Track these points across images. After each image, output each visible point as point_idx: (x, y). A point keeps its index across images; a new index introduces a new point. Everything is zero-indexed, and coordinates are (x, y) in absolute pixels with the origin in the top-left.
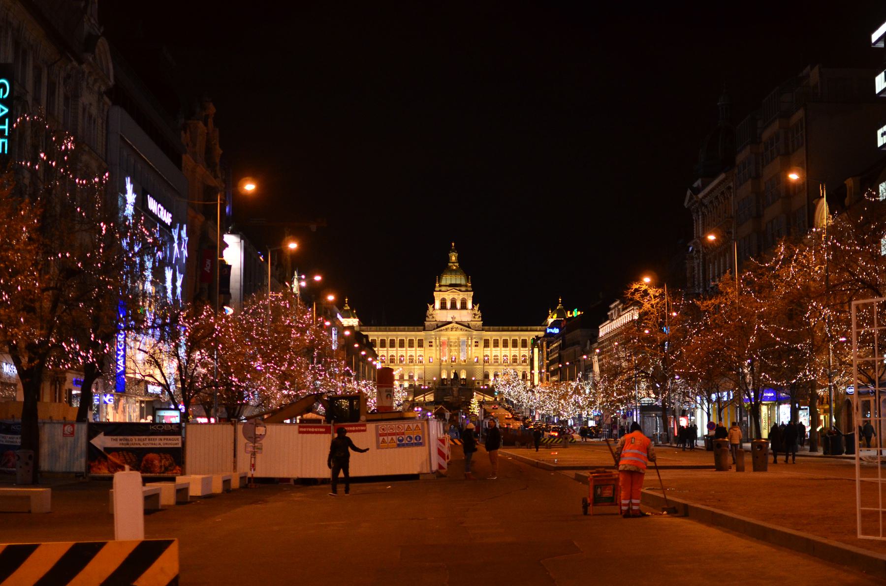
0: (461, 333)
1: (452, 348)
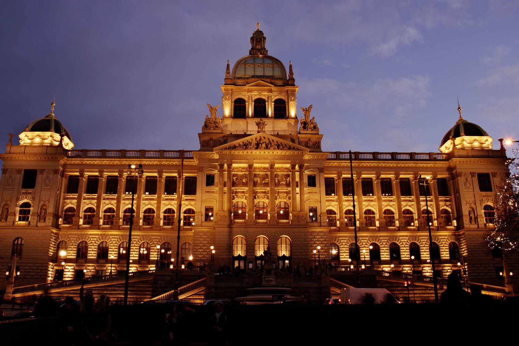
0: (279, 152)
1: (258, 189)
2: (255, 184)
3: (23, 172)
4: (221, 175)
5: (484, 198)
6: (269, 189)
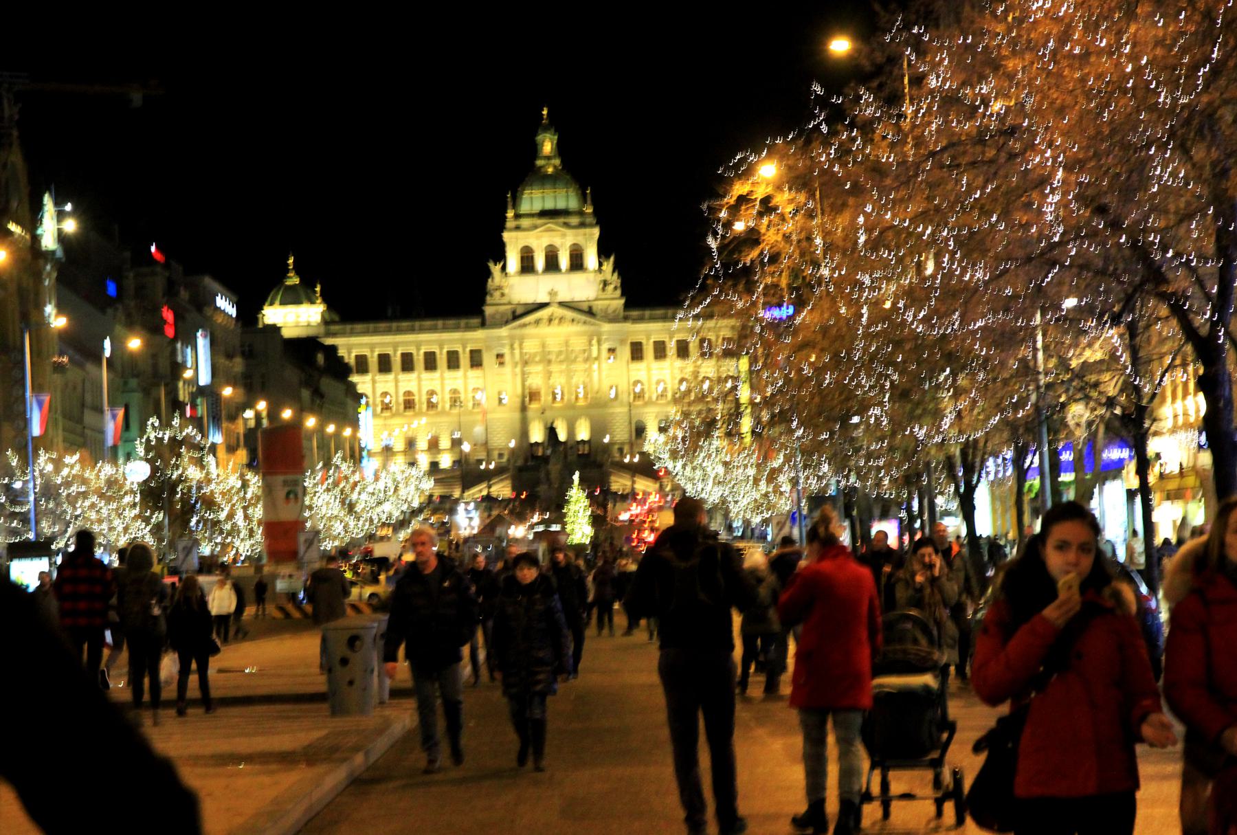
2: (549, 362)
6: (564, 367)
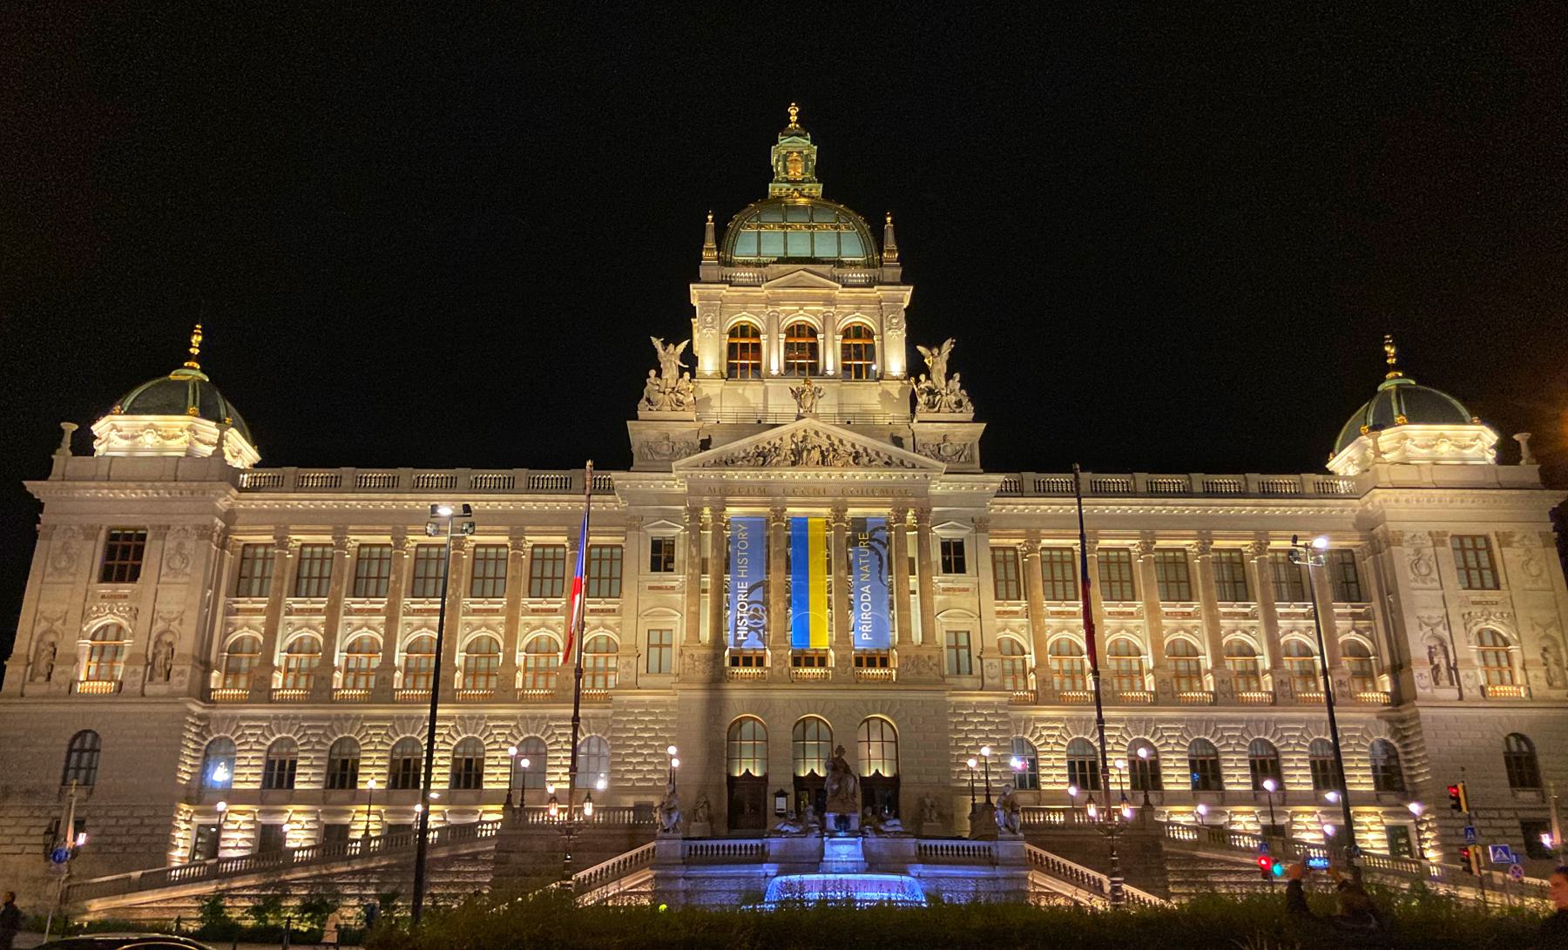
3: (103, 536)
4: (697, 541)
5: (1476, 610)
